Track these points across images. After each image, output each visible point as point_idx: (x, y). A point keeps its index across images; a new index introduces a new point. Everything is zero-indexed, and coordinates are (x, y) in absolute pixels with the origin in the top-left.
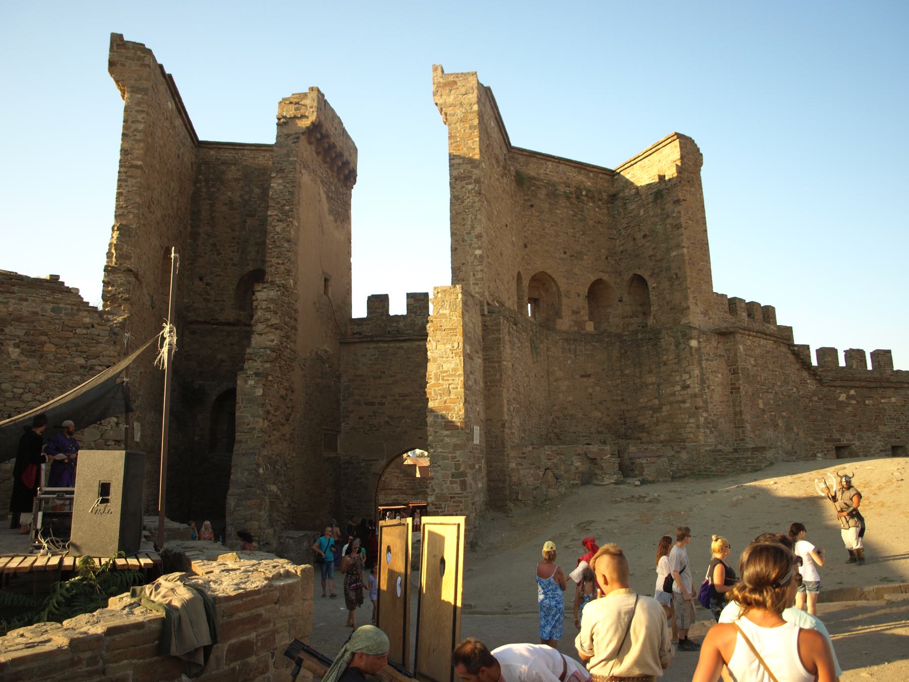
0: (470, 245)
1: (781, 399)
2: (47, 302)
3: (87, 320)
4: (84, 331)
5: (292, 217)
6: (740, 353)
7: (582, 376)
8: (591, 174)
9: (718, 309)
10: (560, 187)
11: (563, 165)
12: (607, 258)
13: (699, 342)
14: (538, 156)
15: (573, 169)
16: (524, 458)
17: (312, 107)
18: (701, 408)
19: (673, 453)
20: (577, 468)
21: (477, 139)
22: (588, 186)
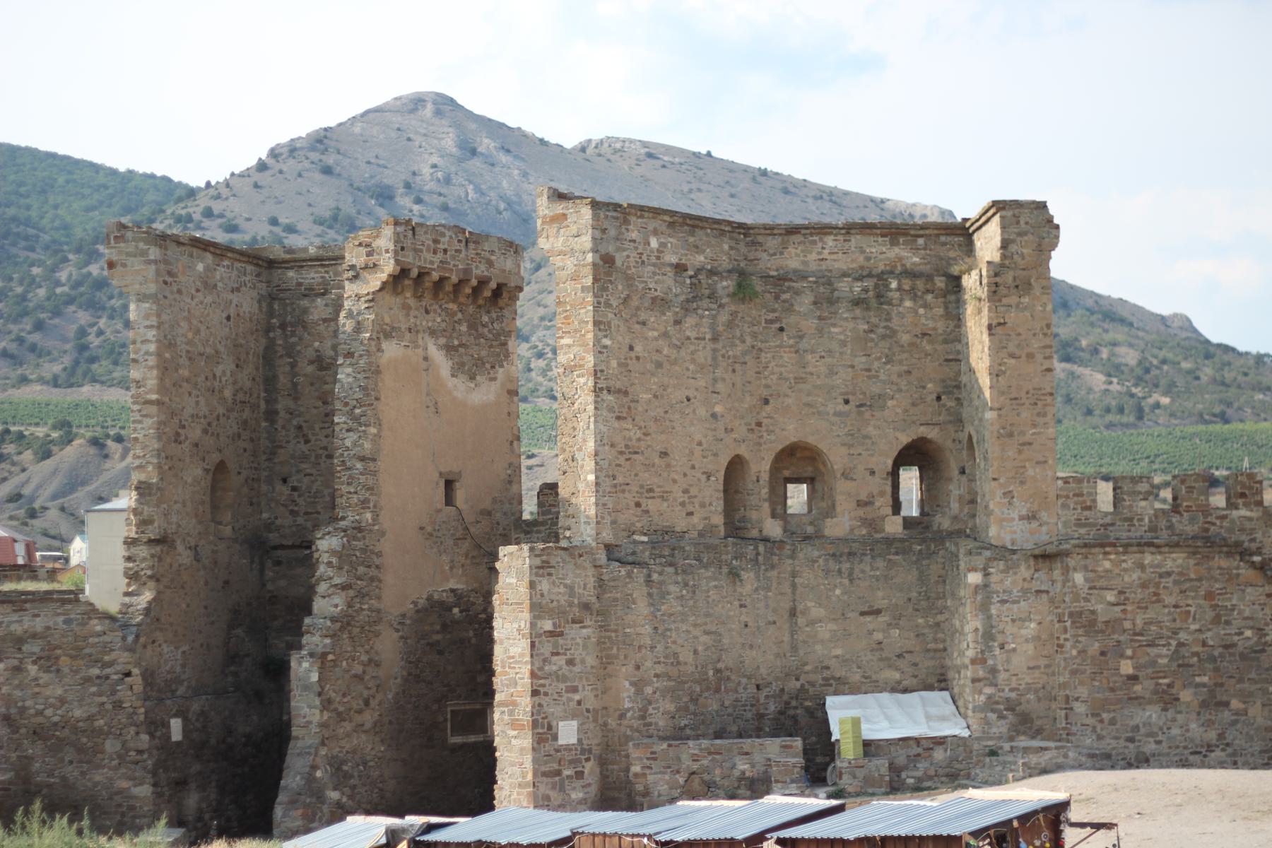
0: (582, 466)
1: (1196, 654)
2: (59, 614)
3: (98, 628)
4: (96, 640)
5: (365, 425)
6: (1075, 586)
7: (863, 614)
8: (921, 241)
9: (1064, 506)
10: (841, 284)
11: (858, 237)
12: (939, 398)
13: (987, 575)
14: (803, 231)
15: (880, 239)
16: (655, 759)
17: (387, 251)
18: (979, 680)
19: (920, 750)
20: (743, 773)
21: (591, 308)
22: (914, 264)
